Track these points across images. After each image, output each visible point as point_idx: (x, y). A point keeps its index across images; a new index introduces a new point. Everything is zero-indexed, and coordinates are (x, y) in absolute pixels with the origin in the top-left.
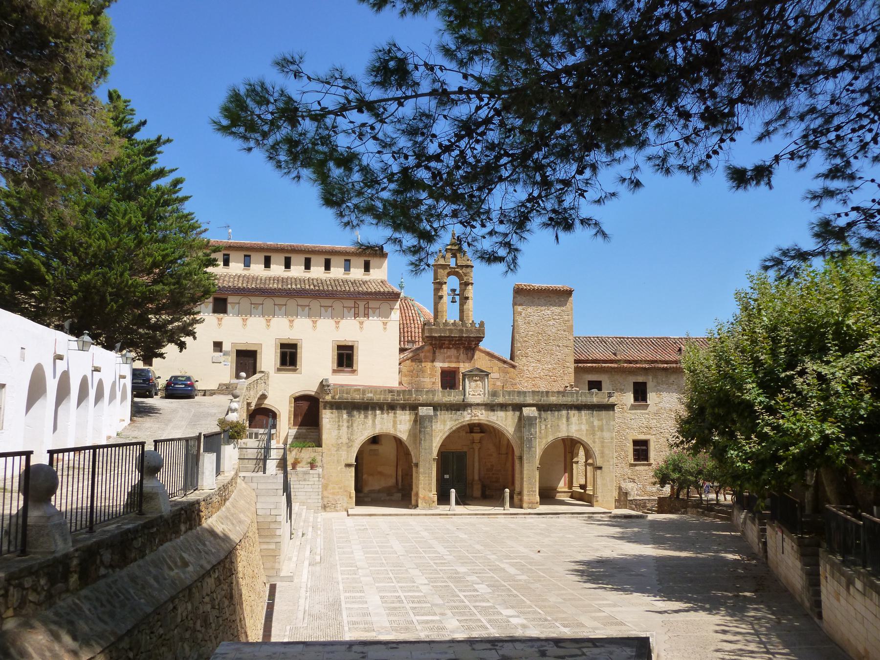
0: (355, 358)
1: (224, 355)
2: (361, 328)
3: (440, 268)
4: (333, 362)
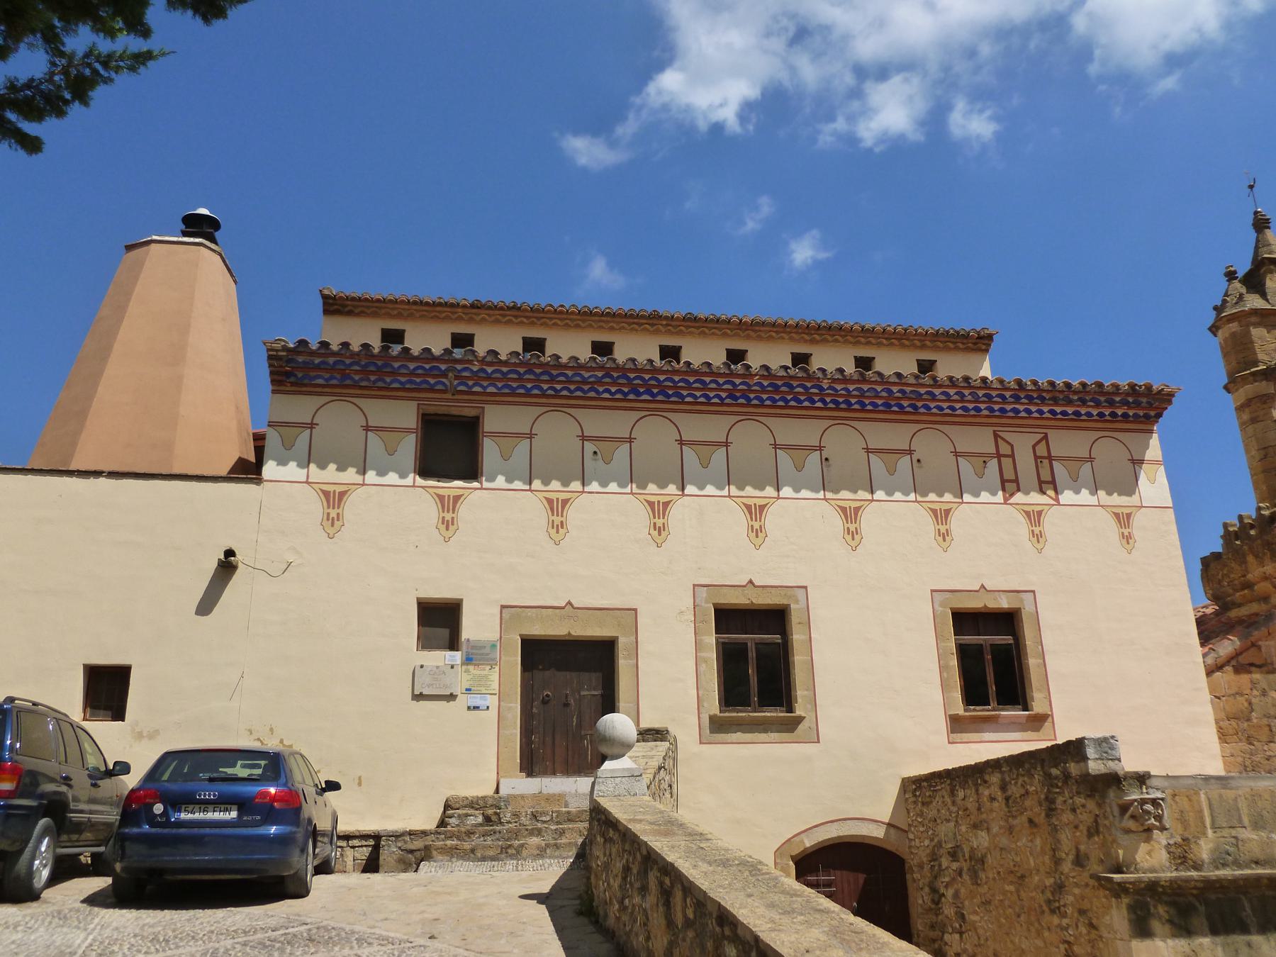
0: (1032, 662)
1: (468, 660)
2: (1038, 537)
3: (1256, 325)
4: (945, 686)
